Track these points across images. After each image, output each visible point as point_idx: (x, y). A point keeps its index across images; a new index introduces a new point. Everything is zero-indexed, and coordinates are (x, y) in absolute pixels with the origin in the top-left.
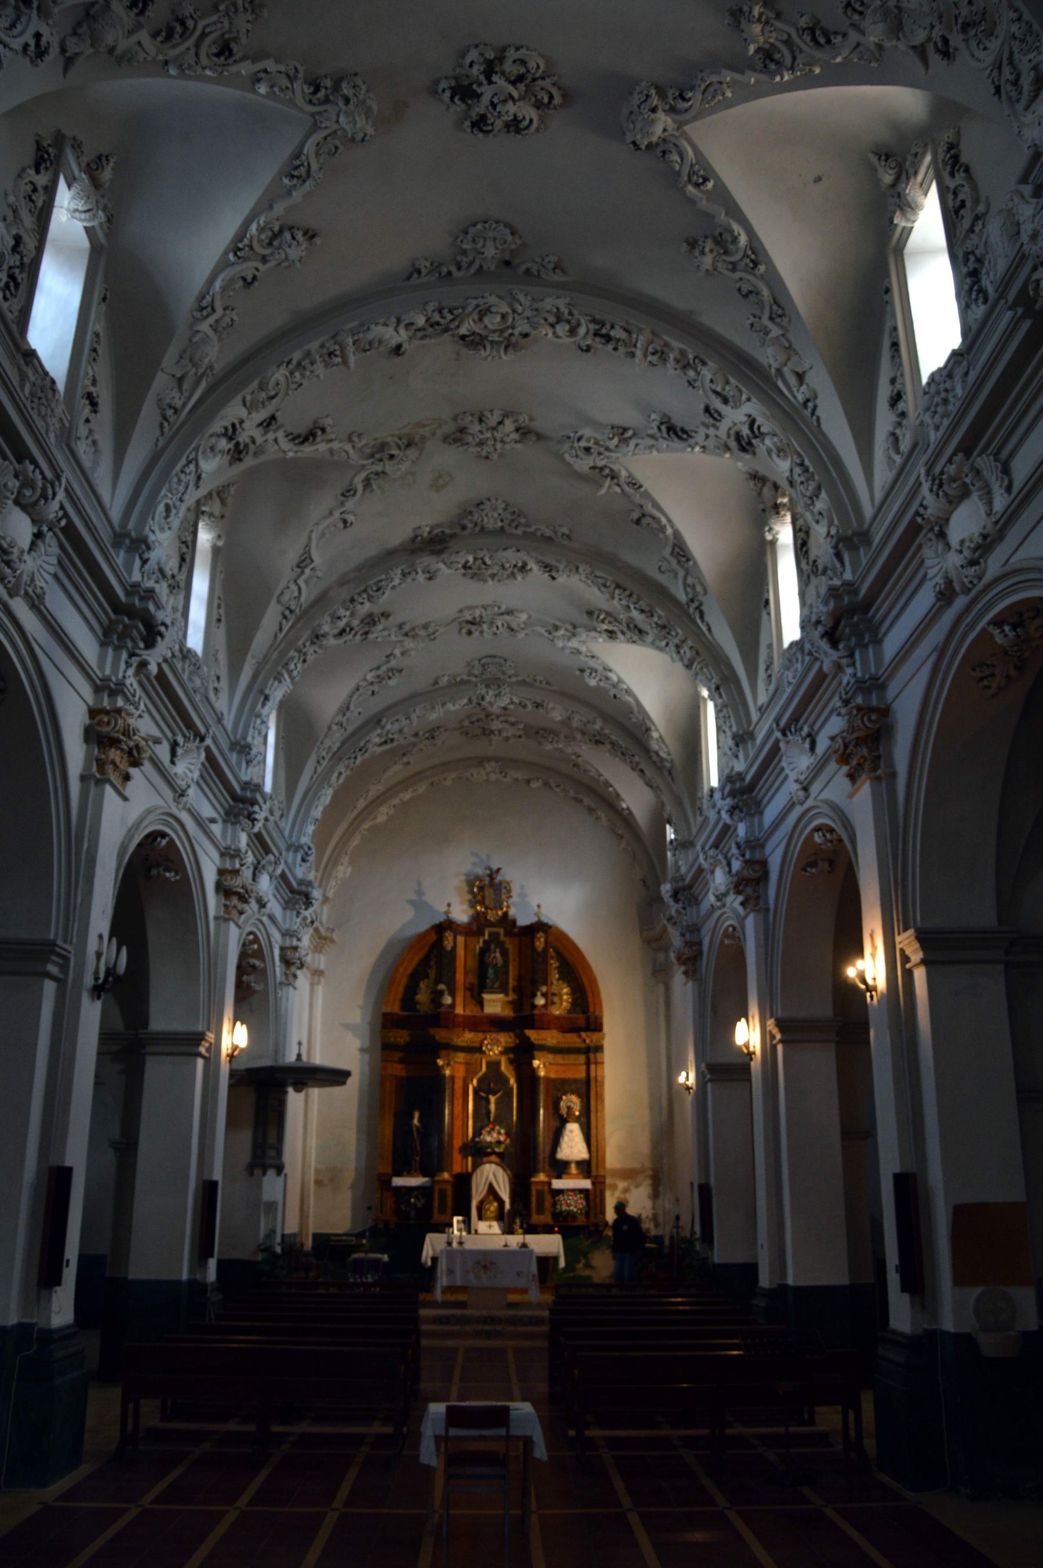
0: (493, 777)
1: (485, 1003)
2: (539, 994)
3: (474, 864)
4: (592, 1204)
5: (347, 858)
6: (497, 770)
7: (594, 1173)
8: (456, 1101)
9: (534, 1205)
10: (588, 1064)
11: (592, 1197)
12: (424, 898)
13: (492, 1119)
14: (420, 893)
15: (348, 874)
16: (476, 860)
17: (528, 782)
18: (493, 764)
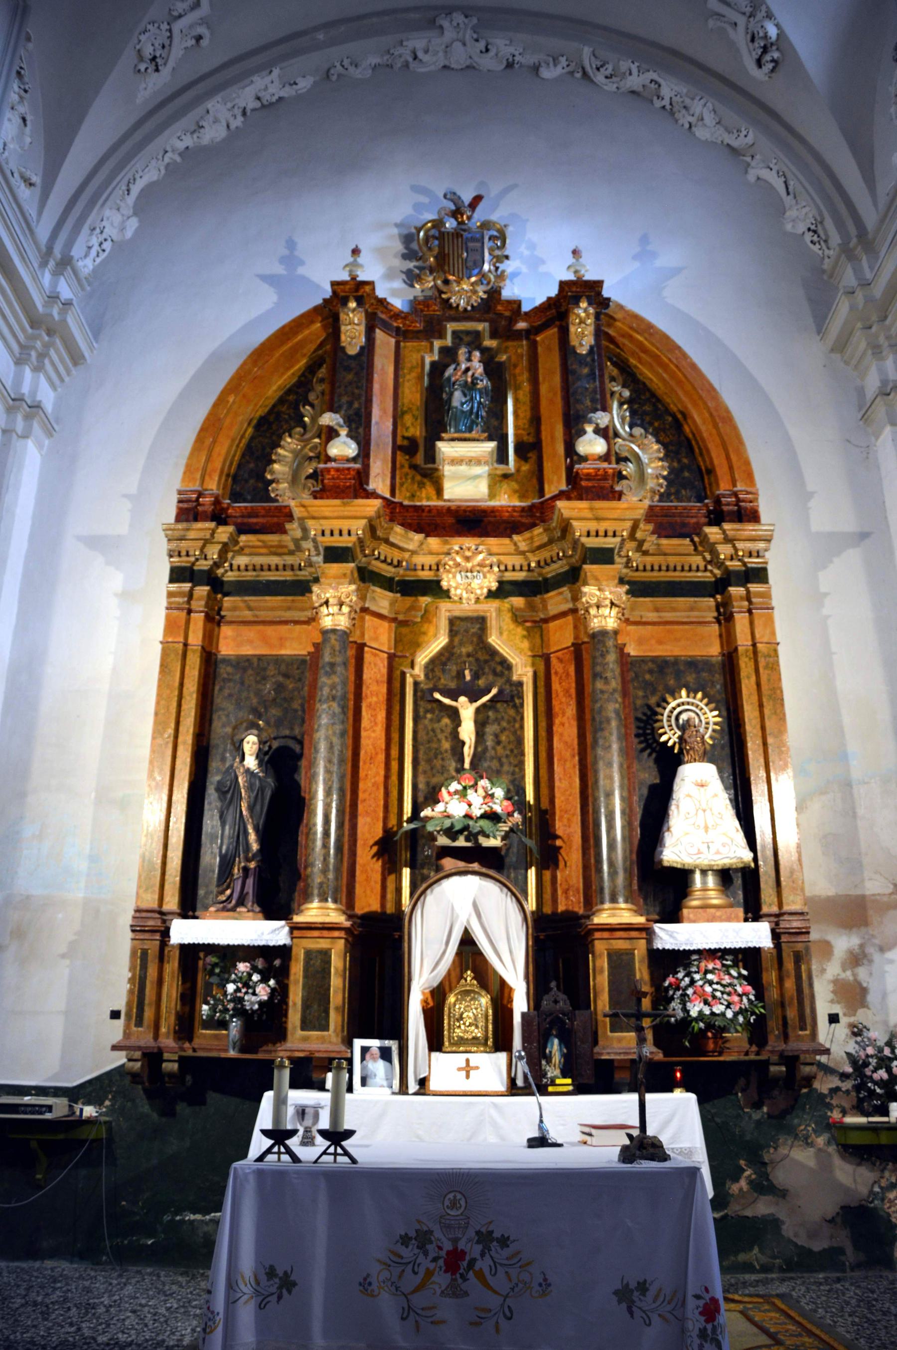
0: (459, 57)
1: (448, 470)
2: (589, 429)
3: (418, 207)
4: (773, 994)
6: (469, 35)
7: (769, 905)
8: (365, 714)
9: (603, 1003)
10: (725, 617)
11: (770, 976)
12: (301, 271)
13: (467, 765)
14: (291, 260)
16: (424, 200)
17: (536, 69)
18: (459, 18)
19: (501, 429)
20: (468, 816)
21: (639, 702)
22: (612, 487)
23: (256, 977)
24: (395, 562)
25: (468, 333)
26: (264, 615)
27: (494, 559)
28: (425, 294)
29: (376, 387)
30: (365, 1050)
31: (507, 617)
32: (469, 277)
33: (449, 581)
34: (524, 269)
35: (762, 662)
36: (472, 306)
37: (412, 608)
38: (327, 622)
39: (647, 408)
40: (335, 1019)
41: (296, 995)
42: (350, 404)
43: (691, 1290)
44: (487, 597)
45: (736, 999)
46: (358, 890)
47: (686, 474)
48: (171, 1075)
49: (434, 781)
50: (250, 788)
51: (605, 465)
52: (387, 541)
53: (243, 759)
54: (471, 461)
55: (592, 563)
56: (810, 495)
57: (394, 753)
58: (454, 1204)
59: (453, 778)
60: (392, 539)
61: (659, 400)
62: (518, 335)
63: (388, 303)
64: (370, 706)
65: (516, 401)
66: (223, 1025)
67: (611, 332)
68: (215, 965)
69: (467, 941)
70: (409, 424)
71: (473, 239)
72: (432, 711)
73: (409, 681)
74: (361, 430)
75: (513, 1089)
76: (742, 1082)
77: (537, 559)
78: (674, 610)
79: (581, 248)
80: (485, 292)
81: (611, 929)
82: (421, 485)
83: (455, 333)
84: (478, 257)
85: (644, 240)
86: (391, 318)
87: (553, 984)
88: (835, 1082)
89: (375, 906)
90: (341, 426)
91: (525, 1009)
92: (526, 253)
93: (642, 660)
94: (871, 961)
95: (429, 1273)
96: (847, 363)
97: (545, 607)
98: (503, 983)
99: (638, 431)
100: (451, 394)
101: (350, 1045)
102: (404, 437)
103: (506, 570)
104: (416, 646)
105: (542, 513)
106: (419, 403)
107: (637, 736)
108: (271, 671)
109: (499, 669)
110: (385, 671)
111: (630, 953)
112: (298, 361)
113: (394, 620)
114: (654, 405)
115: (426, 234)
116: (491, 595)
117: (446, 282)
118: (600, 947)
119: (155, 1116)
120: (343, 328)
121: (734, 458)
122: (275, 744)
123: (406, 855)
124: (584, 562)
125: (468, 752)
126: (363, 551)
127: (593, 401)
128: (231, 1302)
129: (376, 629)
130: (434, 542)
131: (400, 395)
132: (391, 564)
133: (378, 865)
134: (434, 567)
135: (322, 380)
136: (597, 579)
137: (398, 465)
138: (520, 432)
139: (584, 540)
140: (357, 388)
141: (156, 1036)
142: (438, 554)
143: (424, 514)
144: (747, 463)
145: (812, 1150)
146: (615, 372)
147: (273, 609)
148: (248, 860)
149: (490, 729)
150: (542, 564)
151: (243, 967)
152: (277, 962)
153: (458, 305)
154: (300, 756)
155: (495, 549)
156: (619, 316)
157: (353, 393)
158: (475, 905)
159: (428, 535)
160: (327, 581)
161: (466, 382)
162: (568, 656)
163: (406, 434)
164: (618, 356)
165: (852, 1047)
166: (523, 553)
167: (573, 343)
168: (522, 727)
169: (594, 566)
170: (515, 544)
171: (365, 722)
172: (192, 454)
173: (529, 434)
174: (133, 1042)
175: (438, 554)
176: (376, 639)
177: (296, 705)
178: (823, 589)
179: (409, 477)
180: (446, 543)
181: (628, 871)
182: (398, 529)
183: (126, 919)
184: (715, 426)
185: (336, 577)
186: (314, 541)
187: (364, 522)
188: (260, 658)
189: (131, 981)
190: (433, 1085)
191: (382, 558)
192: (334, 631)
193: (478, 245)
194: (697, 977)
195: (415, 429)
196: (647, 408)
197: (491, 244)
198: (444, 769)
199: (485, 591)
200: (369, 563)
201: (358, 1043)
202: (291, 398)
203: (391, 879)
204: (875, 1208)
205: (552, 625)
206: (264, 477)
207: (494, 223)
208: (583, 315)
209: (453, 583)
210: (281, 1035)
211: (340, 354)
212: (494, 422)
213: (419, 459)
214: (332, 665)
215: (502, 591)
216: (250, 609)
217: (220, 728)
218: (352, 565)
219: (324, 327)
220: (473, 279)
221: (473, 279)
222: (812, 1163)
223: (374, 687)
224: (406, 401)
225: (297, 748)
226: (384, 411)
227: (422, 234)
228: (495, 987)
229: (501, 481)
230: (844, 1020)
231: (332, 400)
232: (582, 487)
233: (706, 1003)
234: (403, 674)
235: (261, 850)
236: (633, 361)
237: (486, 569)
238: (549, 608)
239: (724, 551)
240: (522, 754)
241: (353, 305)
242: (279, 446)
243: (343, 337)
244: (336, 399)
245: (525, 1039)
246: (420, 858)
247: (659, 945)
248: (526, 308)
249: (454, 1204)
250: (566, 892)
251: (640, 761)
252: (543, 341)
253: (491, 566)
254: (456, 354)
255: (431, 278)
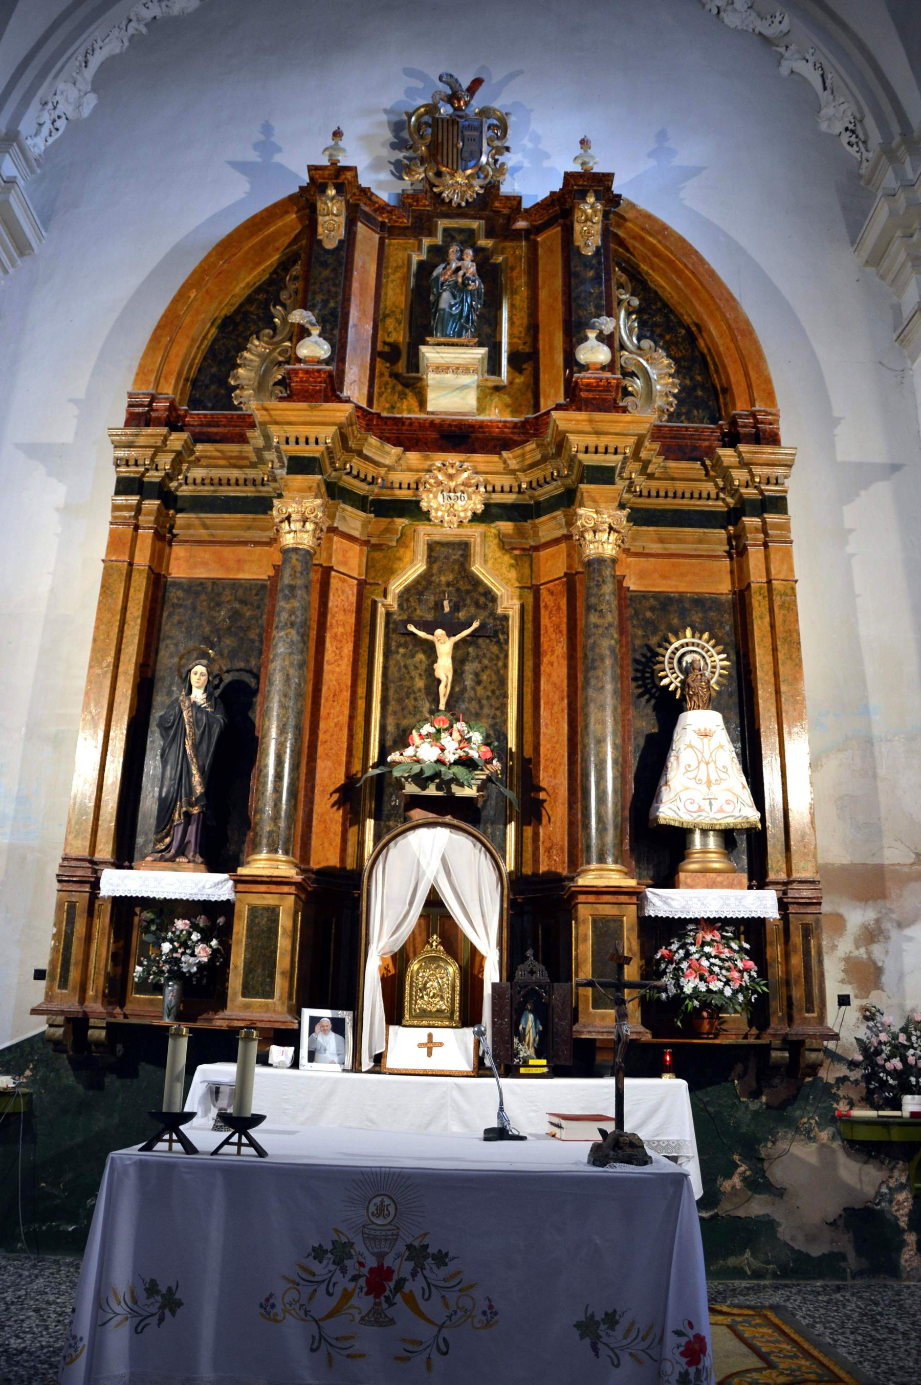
1: (432, 378)
2: (592, 335)
3: (411, 92)
4: (777, 971)
5: (89, 73)
7: (776, 871)
11: (775, 951)
12: (277, 158)
13: (442, 706)
14: (267, 147)
15: (86, 112)
16: (420, 85)
19: (495, 337)
20: (439, 761)
21: (638, 642)
22: (615, 400)
23: (195, 936)
24: (369, 479)
25: (461, 231)
26: (220, 534)
27: (481, 478)
28: (414, 187)
29: (355, 286)
30: (314, 1021)
31: (493, 543)
32: (464, 170)
33: (429, 502)
34: (526, 164)
35: (777, 601)
36: (467, 202)
37: (387, 530)
38: (288, 540)
39: (658, 319)
40: (280, 984)
41: (238, 958)
42: (325, 303)
43: (672, 1324)
44: (470, 521)
45: (736, 975)
46: (315, 842)
47: (700, 393)
48: (98, 1043)
49: (405, 723)
50: (196, 723)
51: (608, 375)
52: (360, 454)
53: (190, 691)
54: (458, 369)
55: (590, 482)
56: (837, 421)
57: (361, 691)
58: (381, 1211)
59: (426, 720)
60: (365, 452)
61: (671, 311)
62: (517, 235)
63: (372, 194)
64: (335, 637)
65: (512, 307)
66: (158, 988)
67: (621, 233)
68: (151, 922)
69: (434, 902)
70: (391, 328)
71: (470, 128)
72: (405, 645)
73: (381, 611)
74: (336, 332)
75: (480, 1070)
76: (739, 1068)
77: (528, 479)
78: (680, 541)
79: (589, 137)
80: (481, 187)
81: (598, 892)
82: (403, 396)
83: (445, 230)
84: (476, 148)
85: (662, 136)
86: (375, 211)
87: (530, 953)
88: (842, 1071)
89: (333, 860)
90: (313, 325)
91: (497, 979)
92: (530, 145)
93: (643, 596)
94: (887, 938)
95: (347, 1295)
96: (882, 277)
97: (536, 534)
98: (474, 950)
99: (647, 344)
100: (439, 295)
101: (299, 1015)
102: (385, 343)
103: (494, 491)
104: (390, 572)
105: (536, 430)
106: (403, 306)
107: (635, 679)
108: (227, 596)
109: (482, 600)
110: (353, 599)
111: (618, 920)
112: (271, 256)
113: (366, 543)
114: (666, 316)
115: (417, 120)
116: (476, 518)
117: (439, 174)
118: (584, 912)
119: (80, 1089)
120: (321, 219)
121: (753, 375)
122: (227, 678)
123: (369, 805)
124: (581, 482)
125: (444, 691)
126: (332, 464)
127: (598, 307)
128: (99, 1324)
129: (345, 552)
130: (413, 457)
131: (383, 298)
132: (364, 480)
133: (338, 815)
134: (413, 486)
135: (296, 278)
136: (594, 501)
137: (377, 374)
138: (516, 340)
139: (581, 456)
140: (334, 285)
141: (82, 1000)
142: (418, 471)
143: (404, 428)
144: (768, 381)
145: (814, 1145)
146: (624, 278)
147: (230, 528)
148: (191, 805)
149: (470, 668)
150: (534, 485)
151: (181, 924)
152: (221, 921)
153: (451, 200)
154: (255, 692)
155: (482, 467)
156: (628, 215)
157: (329, 291)
158: (444, 860)
159: (407, 449)
160: (290, 495)
161: (456, 282)
162: (560, 588)
163: (388, 340)
164: (628, 261)
165: (863, 1033)
166: (513, 472)
167: (577, 244)
168: (506, 666)
169: (592, 486)
170: (505, 462)
171: (329, 655)
172: (146, 354)
173: (525, 343)
174: (55, 1006)
175: (418, 471)
176: (345, 563)
177: (253, 635)
178: (848, 524)
179: (390, 386)
180: (427, 458)
181: (619, 828)
182: (373, 440)
183: (54, 869)
184: (734, 339)
185: (300, 490)
186: (278, 450)
187: (334, 429)
188: (215, 582)
189: (56, 937)
190: (391, 1062)
191: (355, 472)
192: (295, 550)
193: (476, 133)
194: (693, 949)
195: (398, 334)
196: (658, 319)
197: (490, 133)
198: (416, 711)
199: (469, 514)
200: (340, 478)
201: (307, 1013)
202: (261, 297)
203: (353, 831)
204: (882, 1211)
205: (543, 553)
206: (227, 382)
207: (494, 110)
208: (589, 211)
209: (434, 504)
210: (221, 1003)
211: (315, 248)
212: (487, 329)
213: (401, 367)
214: (292, 588)
215: (487, 515)
216: (205, 526)
217: (167, 658)
218: (320, 477)
219: (300, 219)
220: (469, 172)
221: (469, 172)
222: (814, 1160)
223: (340, 617)
224: (389, 303)
225: (252, 682)
226: (363, 312)
227: (413, 119)
228: (465, 955)
229: (491, 394)
230: (855, 1002)
231: (305, 298)
232: (581, 399)
233: (702, 978)
234: (374, 603)
235: (207, 793)
236: (644, 267)
237: (471, 490)
238: (541, 534)
239: (739, 476)
240: (505, 696)
241: (332, 192)
242: (246, 349)
243: (320, 230)
244: (310, 297)
245: (495, 1013)
246: (386, 809)
247: (651, 912)
248: (526, 204)
249: (381, 1211)
250: (549, 850)
251: (636, 707)
252: (544, 241)
253: (477, 487)
254: (446, 253)
255: (421, 170)
